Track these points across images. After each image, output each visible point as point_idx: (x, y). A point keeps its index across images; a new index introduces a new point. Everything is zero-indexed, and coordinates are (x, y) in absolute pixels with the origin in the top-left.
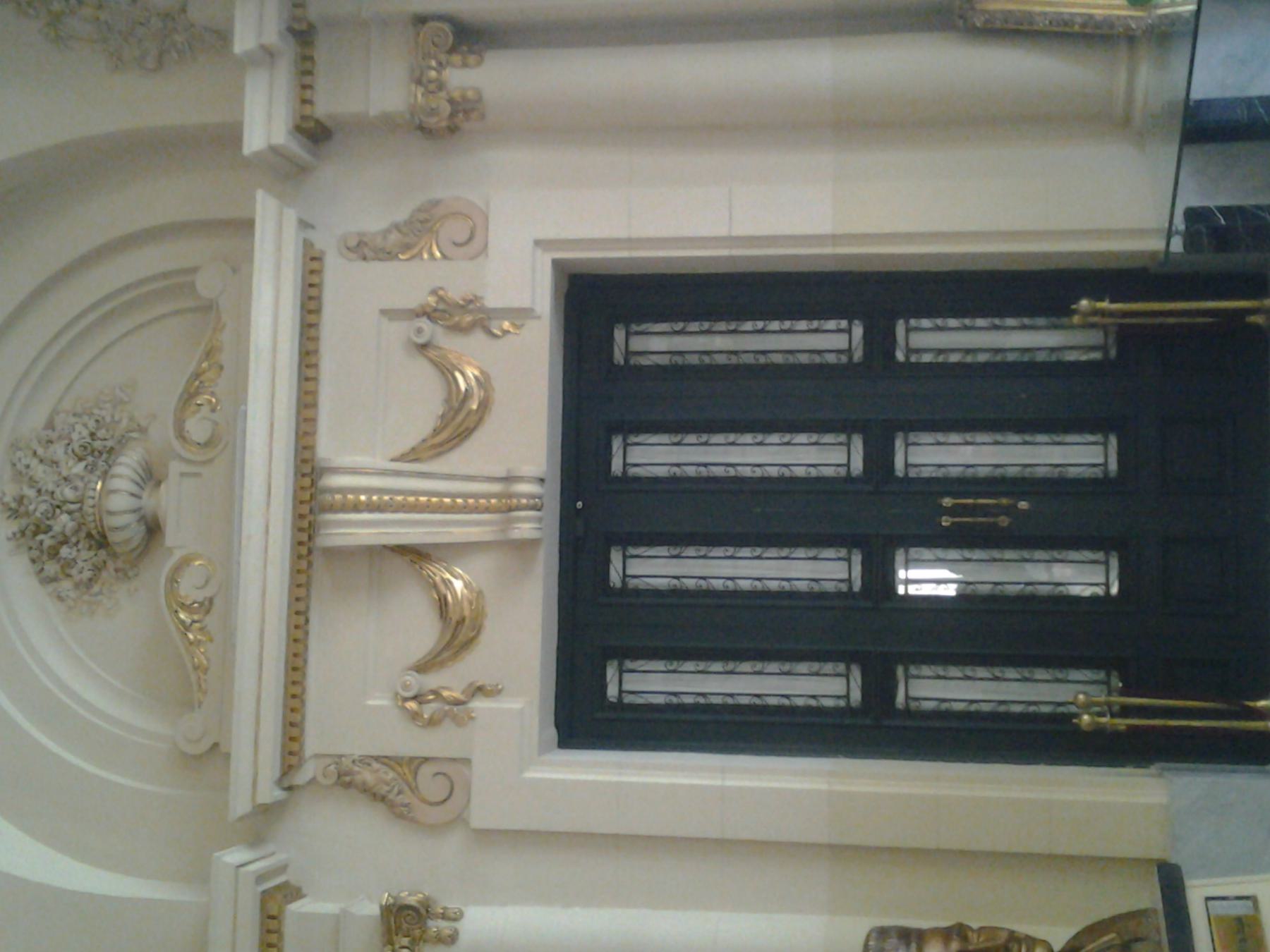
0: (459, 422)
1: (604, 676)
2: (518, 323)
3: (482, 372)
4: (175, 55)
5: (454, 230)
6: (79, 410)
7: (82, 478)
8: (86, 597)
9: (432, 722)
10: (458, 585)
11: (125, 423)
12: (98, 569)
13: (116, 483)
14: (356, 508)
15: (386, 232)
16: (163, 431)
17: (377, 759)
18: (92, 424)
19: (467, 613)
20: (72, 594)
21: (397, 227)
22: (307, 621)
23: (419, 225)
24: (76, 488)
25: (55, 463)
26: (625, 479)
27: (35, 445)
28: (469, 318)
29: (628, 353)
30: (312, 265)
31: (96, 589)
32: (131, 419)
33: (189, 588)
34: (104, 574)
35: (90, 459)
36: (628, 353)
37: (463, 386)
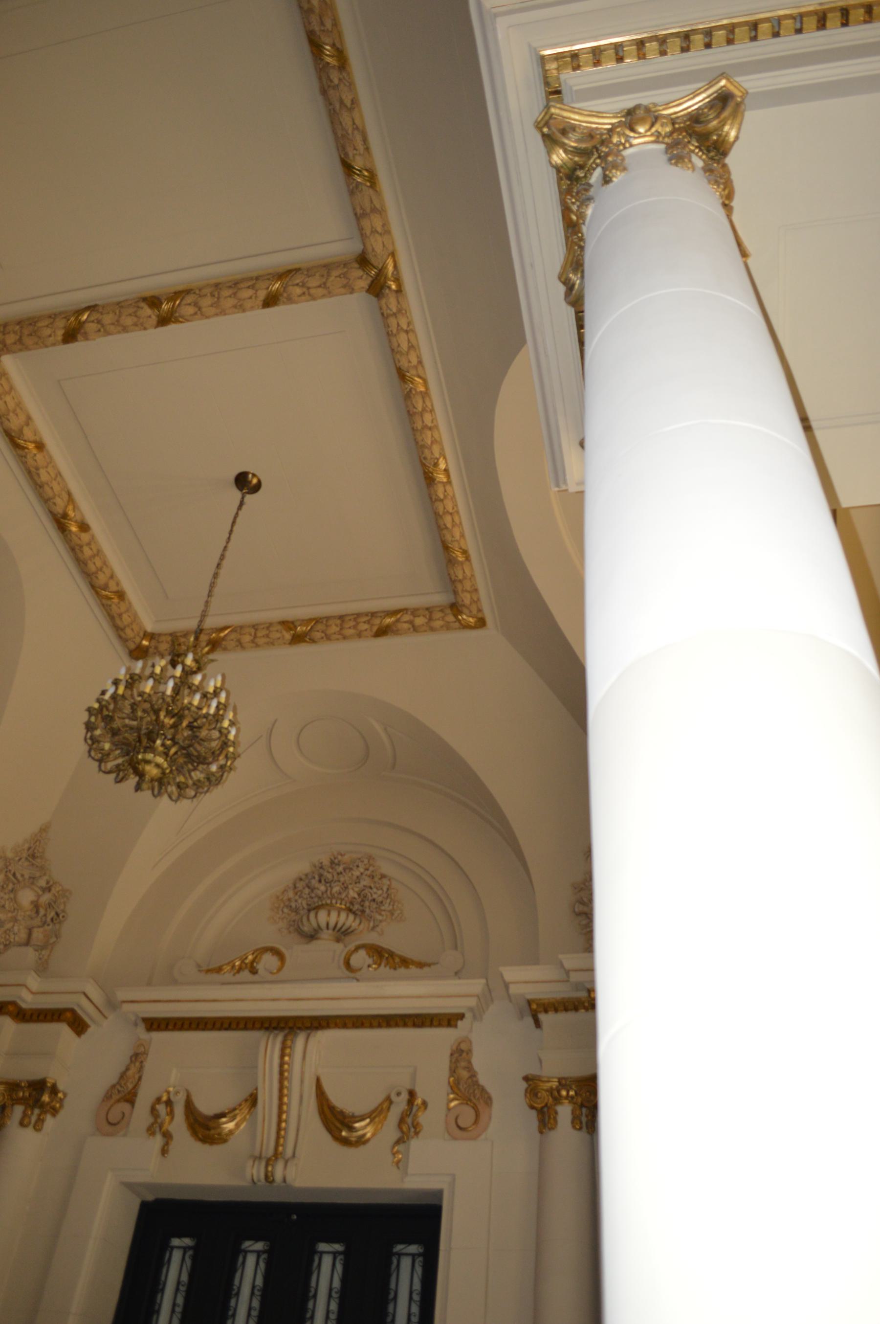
0: (337, 1122)
1: (185, 1236)
2: (400, 1165)
3: (368, 1140)
4: (584, 922)
5: (467, 1116)
6: (389, 892)
7: (347, 896)
8: (282, 905)
9: (153, 1110)
10: (231, 1125)
11: (380, 918)
12: (296, 911)
13: (343, 915)
14: (282, 1056)
15: (469, 1068)
16: (372, 938)
17: (140, 1078)
18: (380, 899)
19: (212, 1132)
20: (285, 898)
21: (473, 1075)
22: (226, 1029)
23: (471, 1091)
24: (340, 893)
25: (358, 880)
26: (313, 1252)
27: (371, 869)
28: (405, 1128)
29: (400, 1255)
30: (450, 1020)
31: (286, 910)
32: (381, 921)
33: (268, 961)
34: (294, 914)
35: (359, 900)
36: (400, 1255)
37: (357, 1125)
